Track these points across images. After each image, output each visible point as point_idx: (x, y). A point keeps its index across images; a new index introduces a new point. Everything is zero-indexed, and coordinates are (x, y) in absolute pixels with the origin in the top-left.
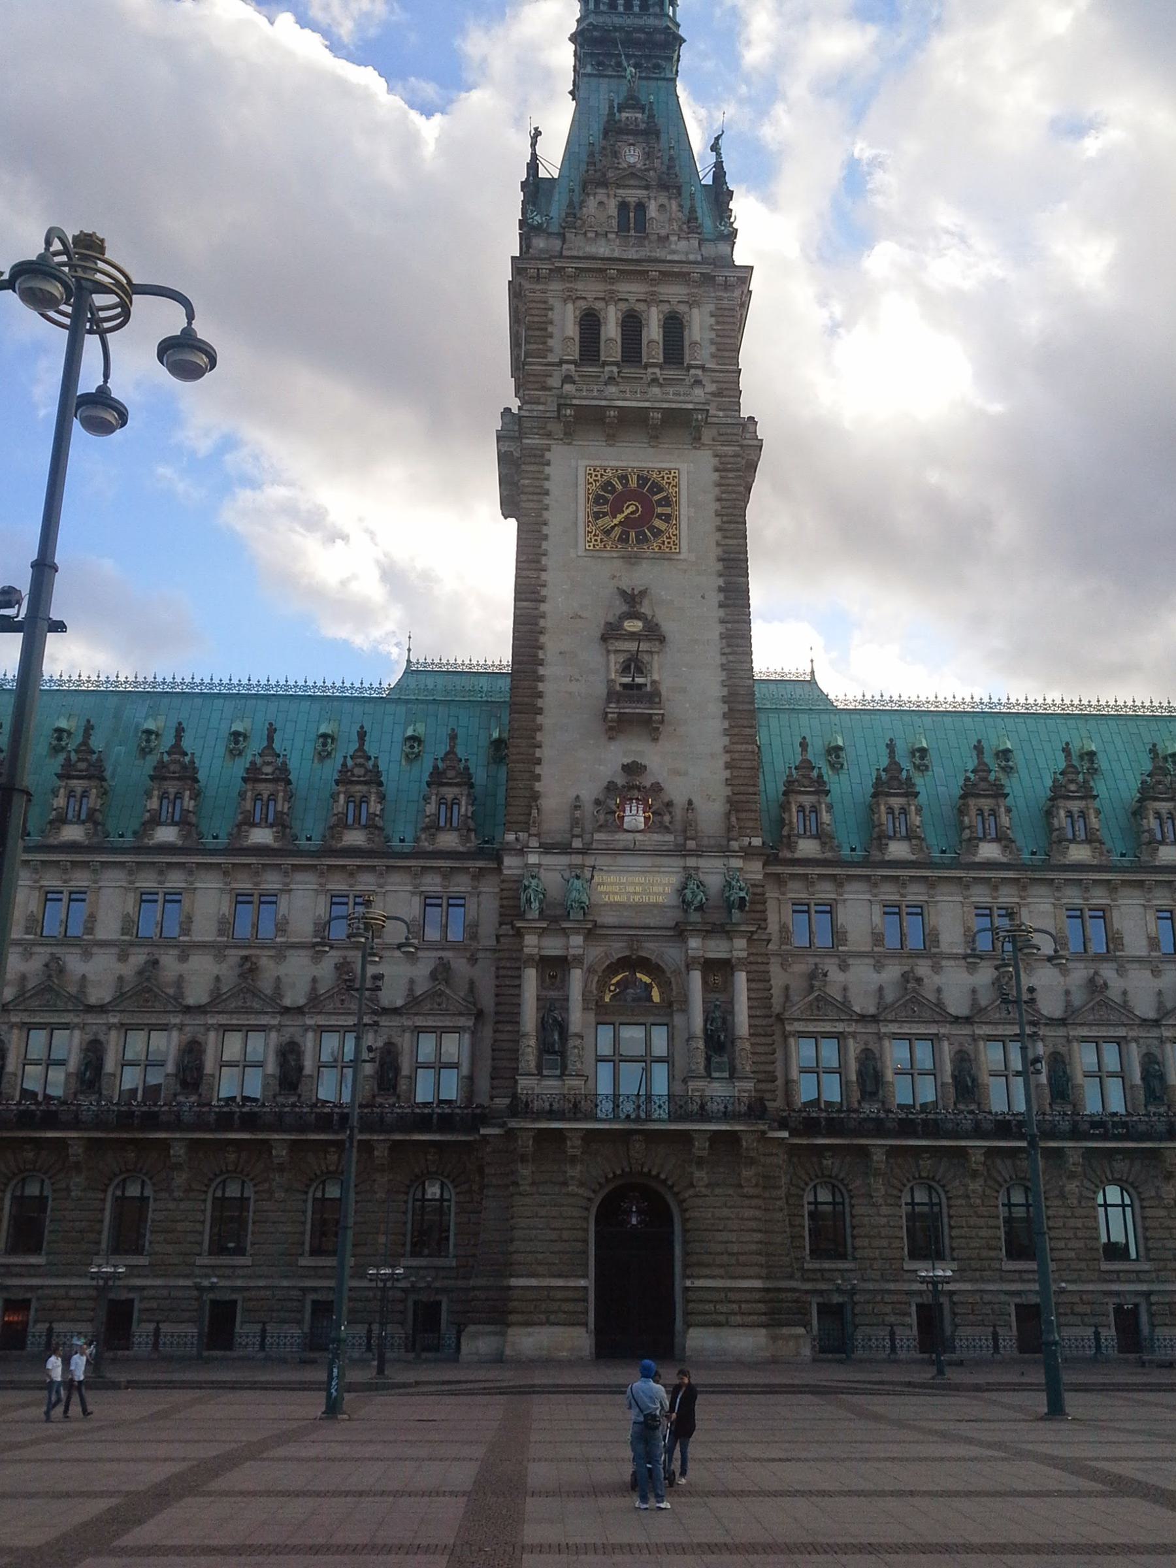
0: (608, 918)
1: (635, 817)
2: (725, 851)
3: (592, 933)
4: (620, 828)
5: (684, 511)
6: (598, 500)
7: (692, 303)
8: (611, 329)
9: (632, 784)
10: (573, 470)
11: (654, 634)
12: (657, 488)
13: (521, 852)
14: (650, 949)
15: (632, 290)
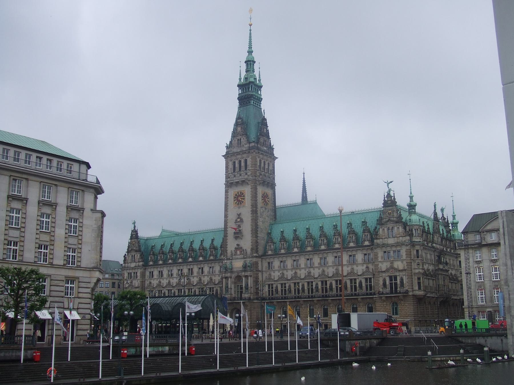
0: (235, 270)
1: (238, 252)
2: (250, 258)
3: (232, 272)
4: (237, 255)
5: (246, 197)
6: (235, 198)
7: (249, 157)
8: (237, 165)
9: (238, 248)
10: (232, 192)
11: (242, 221)
12: (243, 194)
13: (224, 260)
14: (240, 274)
15: (239, 157)
